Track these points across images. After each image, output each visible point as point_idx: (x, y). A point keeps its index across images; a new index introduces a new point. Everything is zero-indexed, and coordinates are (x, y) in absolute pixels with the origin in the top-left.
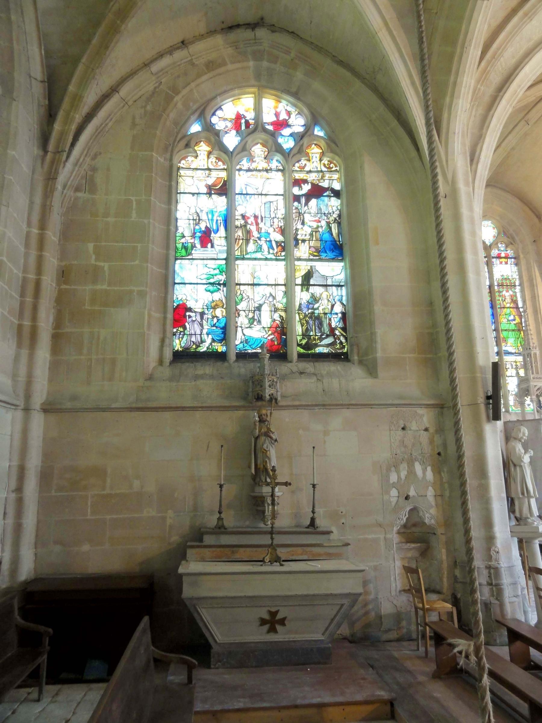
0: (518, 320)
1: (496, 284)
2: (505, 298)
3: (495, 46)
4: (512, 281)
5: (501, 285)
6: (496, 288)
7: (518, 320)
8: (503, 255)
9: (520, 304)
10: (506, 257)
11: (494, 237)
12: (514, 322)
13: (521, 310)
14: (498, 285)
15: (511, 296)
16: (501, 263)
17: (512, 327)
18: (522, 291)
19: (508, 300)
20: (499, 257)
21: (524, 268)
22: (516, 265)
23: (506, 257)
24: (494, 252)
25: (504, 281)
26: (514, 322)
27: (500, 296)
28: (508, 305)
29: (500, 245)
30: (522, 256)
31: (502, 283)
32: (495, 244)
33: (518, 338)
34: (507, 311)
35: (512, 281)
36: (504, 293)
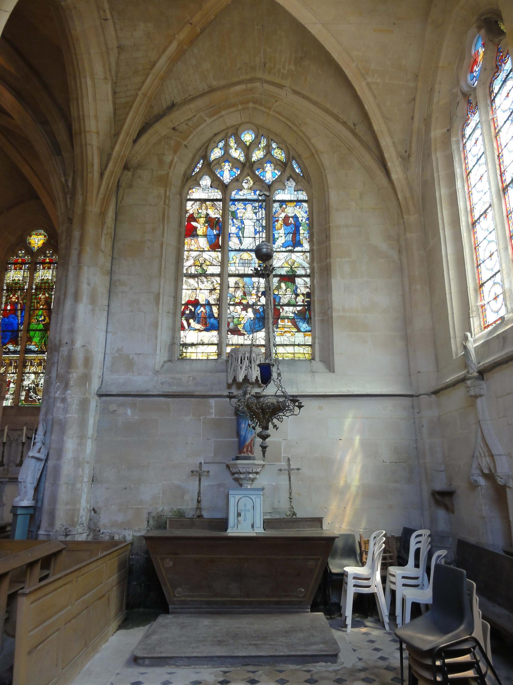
2: (40, 301)
4: (51, 285)
6: (34, 291)
10: (50, 263)
11: (44, 243)
12: (43, 323)
14: (36, 289)
15: (46, 298)
16: (44, 268)
17: (41, 326)
19: (43, 302)
20: (43, 263)
23: (50, 263)
25: (43, 285)
26: (43, 323)
27: (36, 298)
28: (41, 307)
29: (48, 252)
31: (41, 286)
33: (43, 338)
34: (40, 312)
35: (51, 285)
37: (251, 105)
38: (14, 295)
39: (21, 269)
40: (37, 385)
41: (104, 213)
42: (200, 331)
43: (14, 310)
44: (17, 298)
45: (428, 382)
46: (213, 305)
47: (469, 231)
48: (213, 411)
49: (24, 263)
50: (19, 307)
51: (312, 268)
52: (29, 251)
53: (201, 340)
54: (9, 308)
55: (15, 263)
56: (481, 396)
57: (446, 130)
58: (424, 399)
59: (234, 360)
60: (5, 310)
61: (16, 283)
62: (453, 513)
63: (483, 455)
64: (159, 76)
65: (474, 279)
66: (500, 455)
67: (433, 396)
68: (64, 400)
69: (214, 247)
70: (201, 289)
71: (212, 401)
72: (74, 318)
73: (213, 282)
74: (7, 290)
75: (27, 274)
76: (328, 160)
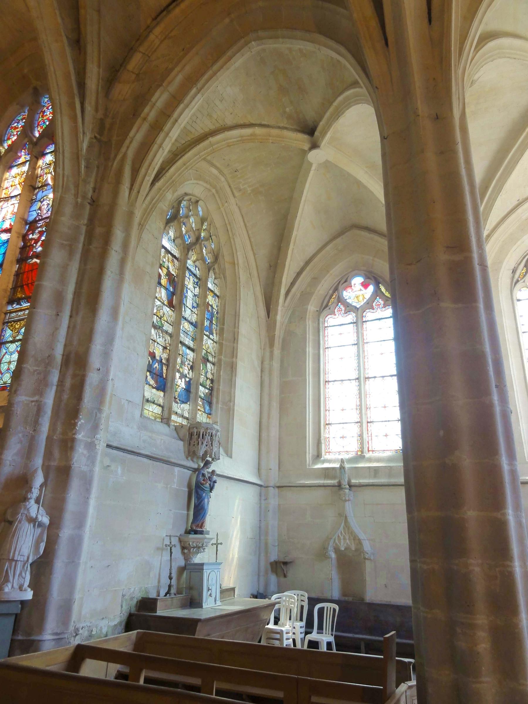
37: (214, 191)
41: (142, 226)
42: (153, 388)
45: (274, 478)
46: (164, 364)
47: (324, 385)
48: (175, 480)
51: (220, 360)
53: (153, 399)
56: (349, 500)
57: (316, 309)
58: (271, 490)
59: (208, 435)
62: (285, 576)
63: (342, 538)
64: (228, 141)
65: (324, 418)
66: (365, 540)
67: (277, 489)
69: (171, 305)
70: (158, 343)
71: (177, 469)
72: (110, 340)
73: (165, 340)
76: (243, 276)
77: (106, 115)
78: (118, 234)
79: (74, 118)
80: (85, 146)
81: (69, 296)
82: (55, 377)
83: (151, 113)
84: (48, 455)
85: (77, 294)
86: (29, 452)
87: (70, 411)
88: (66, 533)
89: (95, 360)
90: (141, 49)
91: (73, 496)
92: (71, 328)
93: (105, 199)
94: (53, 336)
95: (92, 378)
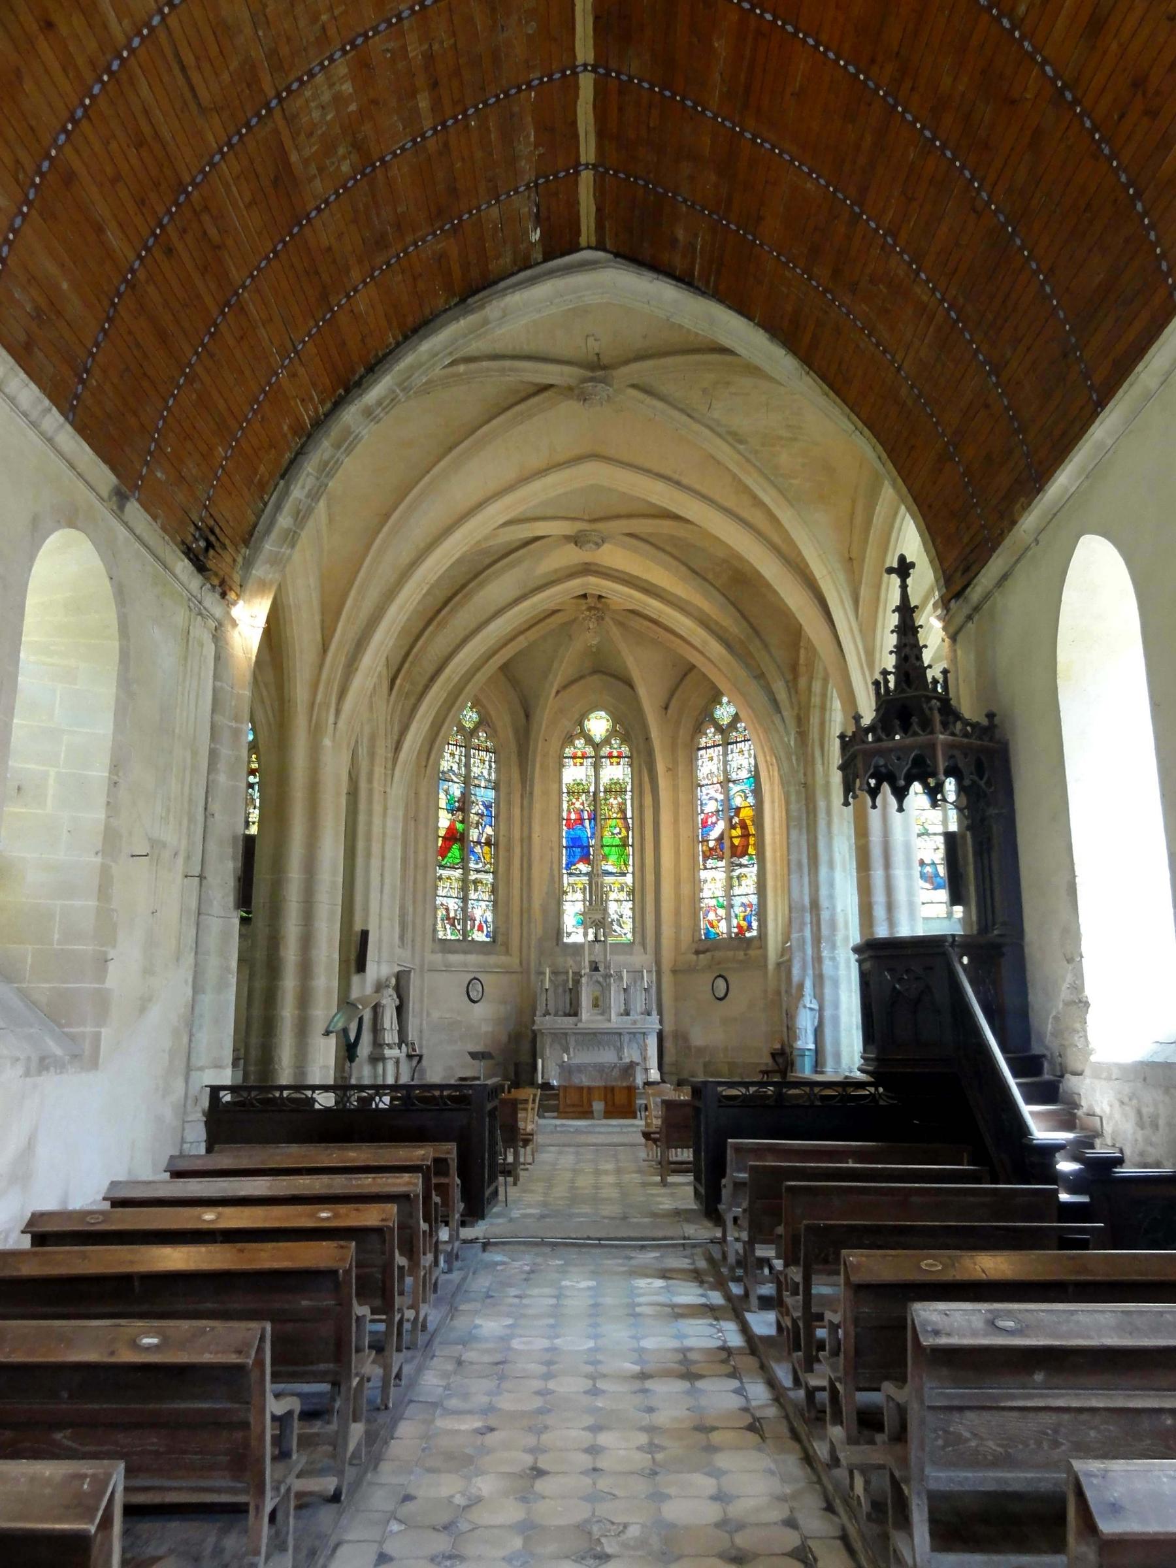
0: (624, 833)
1: (602, 789)
3: (415, 650)
5: (608, 791)
6: (602, 794)
7: (624, 833)
8: (615, 754)
9: (629, 814)
10: (619, 757)
13: (630, 821)
14: (605, 792)
15: (619, 804)
16: (612, 764)
17: (617, 841)
18: (632, 799)
20: (610, 756)
21: (636, 769)
22: (631, 765)
23: (619, 757)
24: (605, 751)
30: (635, 755)
32: (606, 741)
34: (613, 822)
36: (612, 800)
38: (577, 799)
39: (582, 764)
40: (621, 916)
43: (582, 819)
44: (583, 804)
49: (584, 757)
50: (586, 816)
52: (589, 740)
54: (573, 816)
55: (574, 757)
60: (568, 820)
61: (578, 784)
68: (833, 959)
72: (832, 885)
74: (568, 793)
75: (591, 772)
77: (800, 709)
78: (821, 804)
79: (777, 731)
80: (792, 743)
81: (805, 861)
82: (808, 919)
83: (816, 700)
84: (814, 968)
85: (809, 858)
86: (804, 968)
87: (817, 940)
88: (828, 1013)
89: (824, 902)
90: (802, 644)
91: (828, 991)
92: (810, 882)
93: (810, 781)
94: (801, 892)
95: (825, 915)
